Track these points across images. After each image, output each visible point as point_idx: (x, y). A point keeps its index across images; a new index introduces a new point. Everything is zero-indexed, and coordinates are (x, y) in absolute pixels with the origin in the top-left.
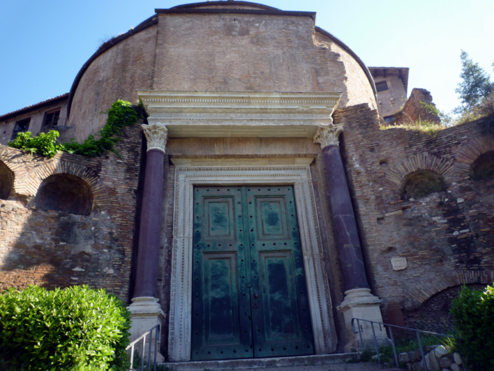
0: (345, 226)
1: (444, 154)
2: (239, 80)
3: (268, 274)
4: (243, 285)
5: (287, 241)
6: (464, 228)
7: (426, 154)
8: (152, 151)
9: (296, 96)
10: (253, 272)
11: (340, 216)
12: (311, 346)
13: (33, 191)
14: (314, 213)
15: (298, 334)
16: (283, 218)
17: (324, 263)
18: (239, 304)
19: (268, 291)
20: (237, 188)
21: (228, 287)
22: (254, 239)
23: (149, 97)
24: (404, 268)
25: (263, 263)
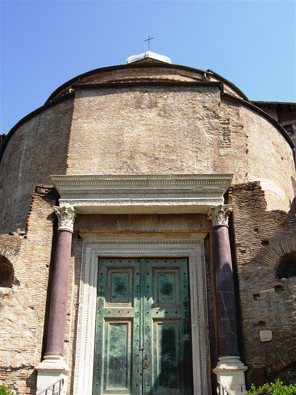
2: (145, 154)
3: (161, 338)
5: (178, 311)
9: (191, 178)
10: (146, 337)
11: (221, 292)
15: (181, 389)
16: (176, 288)
23: (60, 181)
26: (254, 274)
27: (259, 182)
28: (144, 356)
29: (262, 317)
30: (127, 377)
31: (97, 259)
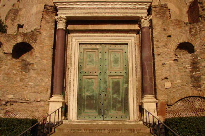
0: (146, 67)
1: (197, 35)
3: (112, 86)
4: (100, 90)
6: (198, 71)
7: (188, 34)
8: (59, 29)
10: (105, 85)
11: (145, 62)
13: (11, 51)
14: (136, 59)
15: (123, 112)
16: (121, 60)
18: (98, 98)
19: (111, 93)
20: (100, 45)
21: (94, 91)
22: (106, 70)
24: (169, 87)
25: (110, 81)
26: (163, 53)
27: (167, 4)
29: (166, 76)
31: (78, 44)
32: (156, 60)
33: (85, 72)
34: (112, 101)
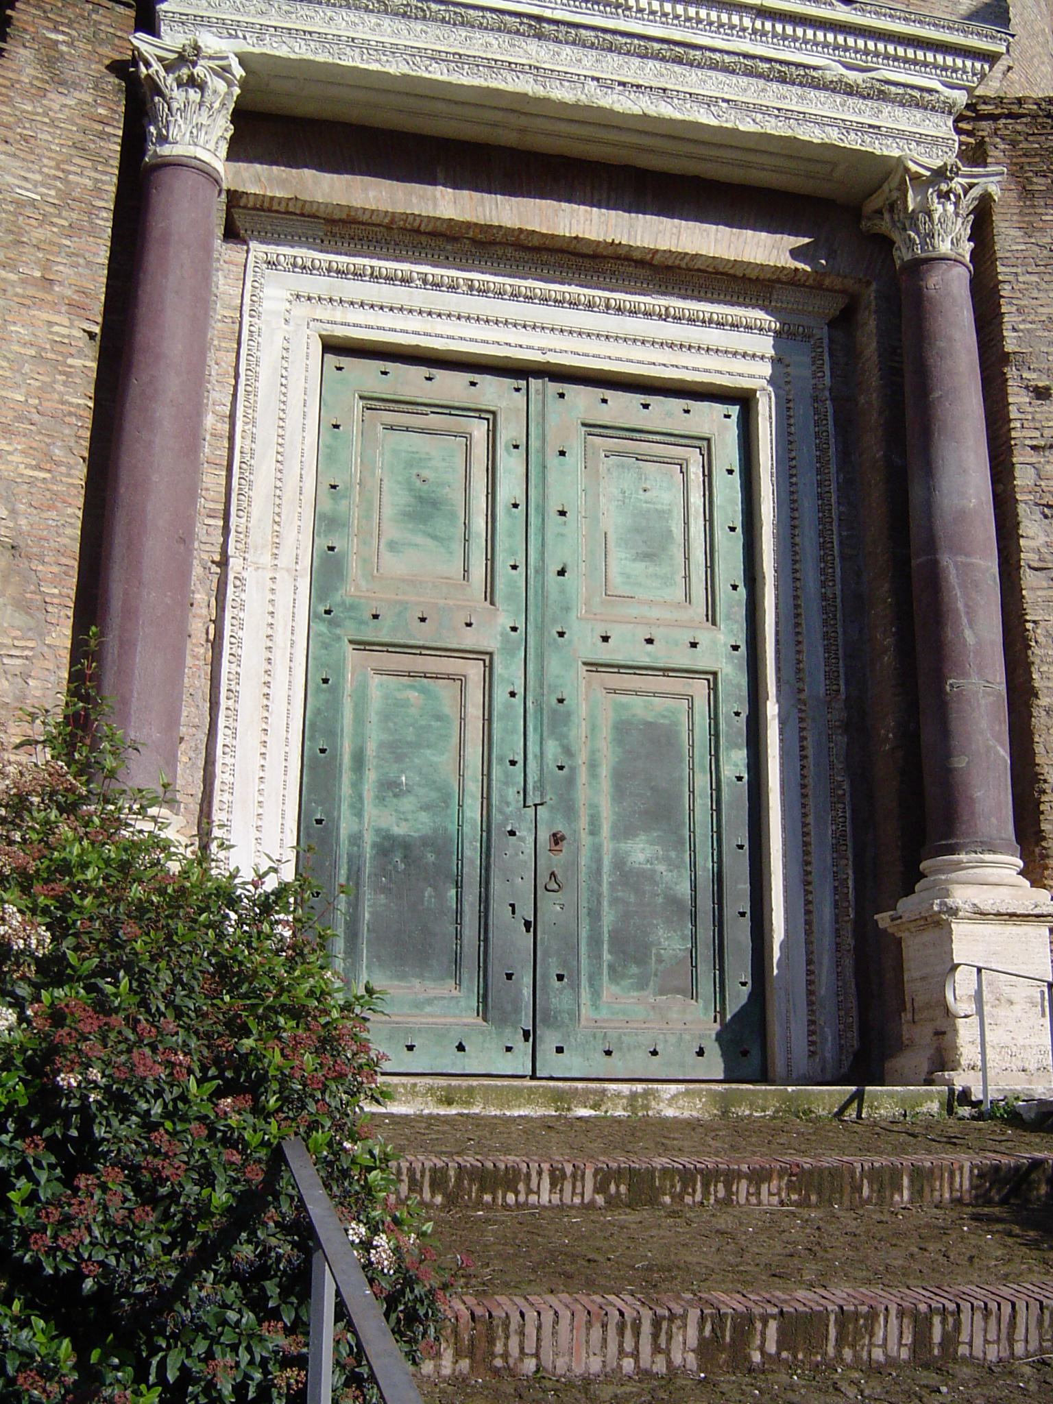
10: (552, 747)
12: (755, 1052)
17: (842, 740)
20: (510, 383)
22: (567, 609)
28: (544, 836)
30: (458, 935)
32: (1031, 556)
33: (376, 617)
34: (614, 901)
